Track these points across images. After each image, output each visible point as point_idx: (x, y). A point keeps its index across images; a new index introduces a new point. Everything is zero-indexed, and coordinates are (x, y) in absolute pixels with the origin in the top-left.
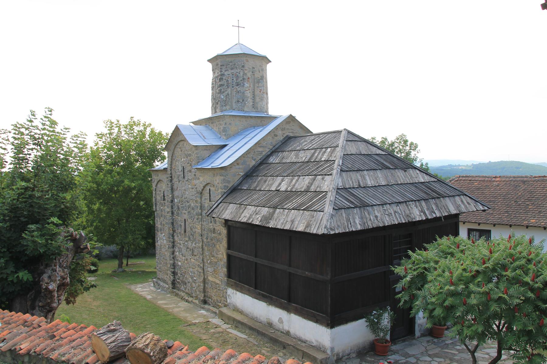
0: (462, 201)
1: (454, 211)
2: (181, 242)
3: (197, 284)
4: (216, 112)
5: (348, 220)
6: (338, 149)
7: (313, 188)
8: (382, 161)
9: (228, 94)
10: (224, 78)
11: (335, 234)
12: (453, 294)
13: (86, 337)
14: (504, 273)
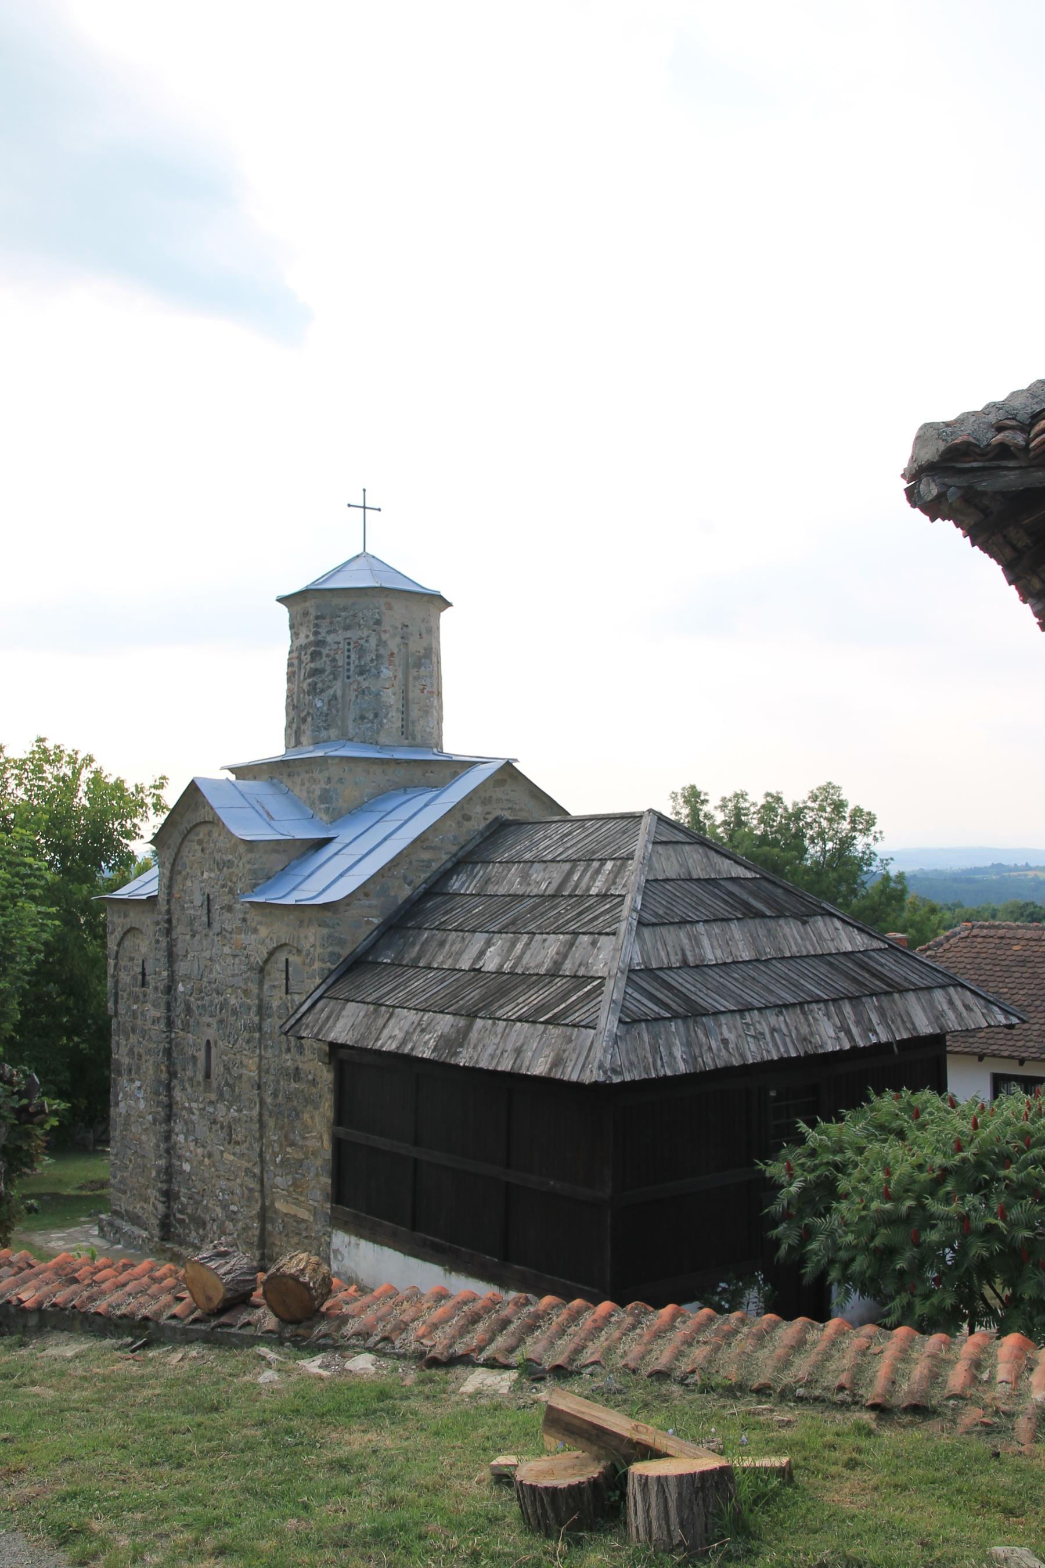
0: (951, 1003)
1: (925, 1027)
2: (194, 1105)
3: (240, 1225)
4: (298, 743)
5: (655, 1049)
6: (632, 865)
7: (568, 968)
8: (745, 896)
9: (335, 697)
10: (325, 651)
11: (623, 1083)
12: (888, 1220)
13: (146, 1279)
14: (1002, 1173)
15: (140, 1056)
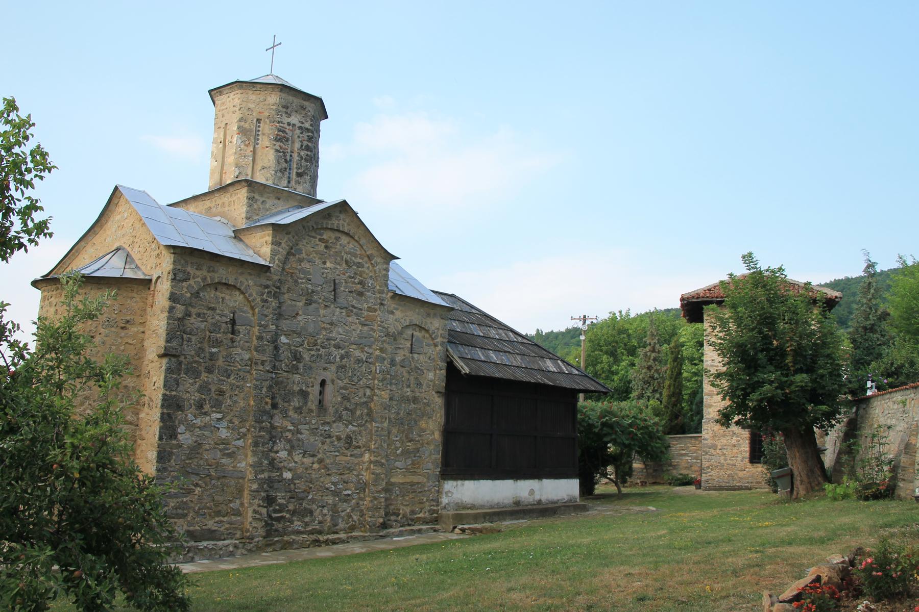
15: (221, 393)
